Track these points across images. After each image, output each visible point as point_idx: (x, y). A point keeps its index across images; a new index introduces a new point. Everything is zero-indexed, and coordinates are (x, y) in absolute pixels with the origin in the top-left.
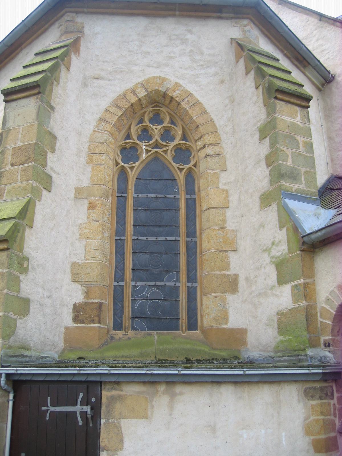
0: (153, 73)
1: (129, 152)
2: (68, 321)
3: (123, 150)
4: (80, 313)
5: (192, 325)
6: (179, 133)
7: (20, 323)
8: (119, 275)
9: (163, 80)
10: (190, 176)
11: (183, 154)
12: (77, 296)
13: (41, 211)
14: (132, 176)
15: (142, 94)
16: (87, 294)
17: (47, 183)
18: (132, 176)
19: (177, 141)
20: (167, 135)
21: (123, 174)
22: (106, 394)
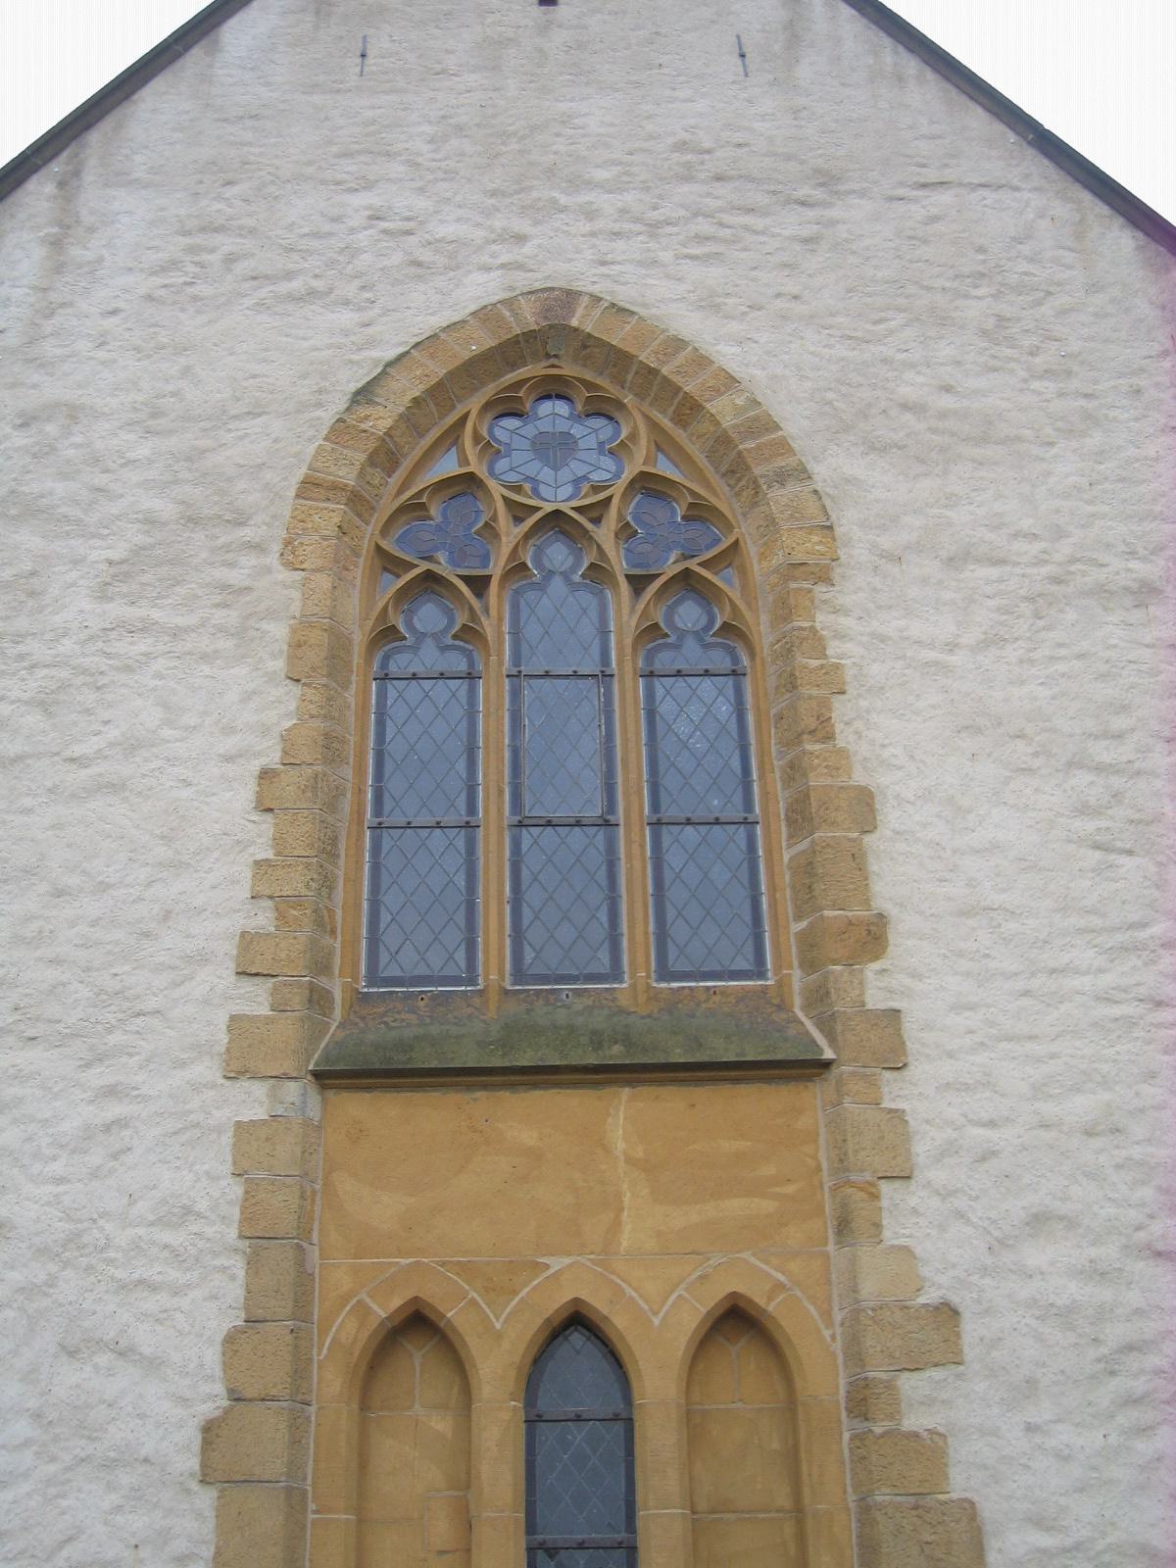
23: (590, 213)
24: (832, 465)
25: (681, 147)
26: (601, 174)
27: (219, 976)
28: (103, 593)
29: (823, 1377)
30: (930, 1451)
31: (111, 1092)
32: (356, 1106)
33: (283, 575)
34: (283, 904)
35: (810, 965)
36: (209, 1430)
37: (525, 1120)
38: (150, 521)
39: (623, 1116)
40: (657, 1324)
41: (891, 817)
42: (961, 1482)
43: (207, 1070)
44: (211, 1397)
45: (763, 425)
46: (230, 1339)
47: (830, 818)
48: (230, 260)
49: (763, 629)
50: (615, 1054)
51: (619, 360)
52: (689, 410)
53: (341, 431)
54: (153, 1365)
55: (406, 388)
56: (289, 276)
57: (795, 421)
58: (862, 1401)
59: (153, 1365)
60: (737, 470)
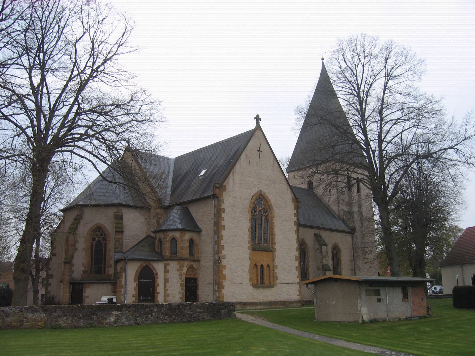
0: (98, 222)
1: (94, 239)
2: (82, 273)
3: (93, 239)
4: (84, 272)
5: (105, 273)
6: (103, 234)
7: (72, 275)
8: (92, 264)
9: (100, 223)
10: (105, 244)
11: (104, 239)
12: (83, 269)
13: (75, 256)
14: (94, 244)
15: (95, 227)
16: (85, 268)
17: (76, 250)
18: (94, 244)
19: (103, 236)
20: (101, 235)
21: (92, 244)
22: (84, 285)
23: (263, 183)
24: (275, 209)
25: (268, 177)
26: (263, 179)
27: (247, 243)
28: (239, 214)
29: (272, 269)
30: (276, 273)
31: (243, 250)
32: (254, 252)
33: (248, 214)
34: (250, 239)
35: (272, 244)
36: (249, 270)
37: (260, 253)
38: (241, 208)
39: (264, 254)
40: (265, 266)
41: (276, 236)
42: (277, 275)
43: (247, 249)
44: (249, 268)
45: (271, 205)
46: (250, 265)
47: (273, 235)
48: (243, 184)
49: (270, 220)
50: (264, 250)
51: (264, 197)
52: (267, 202)
53: (251, 202)
54: (246, 266)
55: (254, 199)
56: (247, 186)
57: (273, 205)
58: (273, 270)
59: (246, 266)
60: (270, 208)
